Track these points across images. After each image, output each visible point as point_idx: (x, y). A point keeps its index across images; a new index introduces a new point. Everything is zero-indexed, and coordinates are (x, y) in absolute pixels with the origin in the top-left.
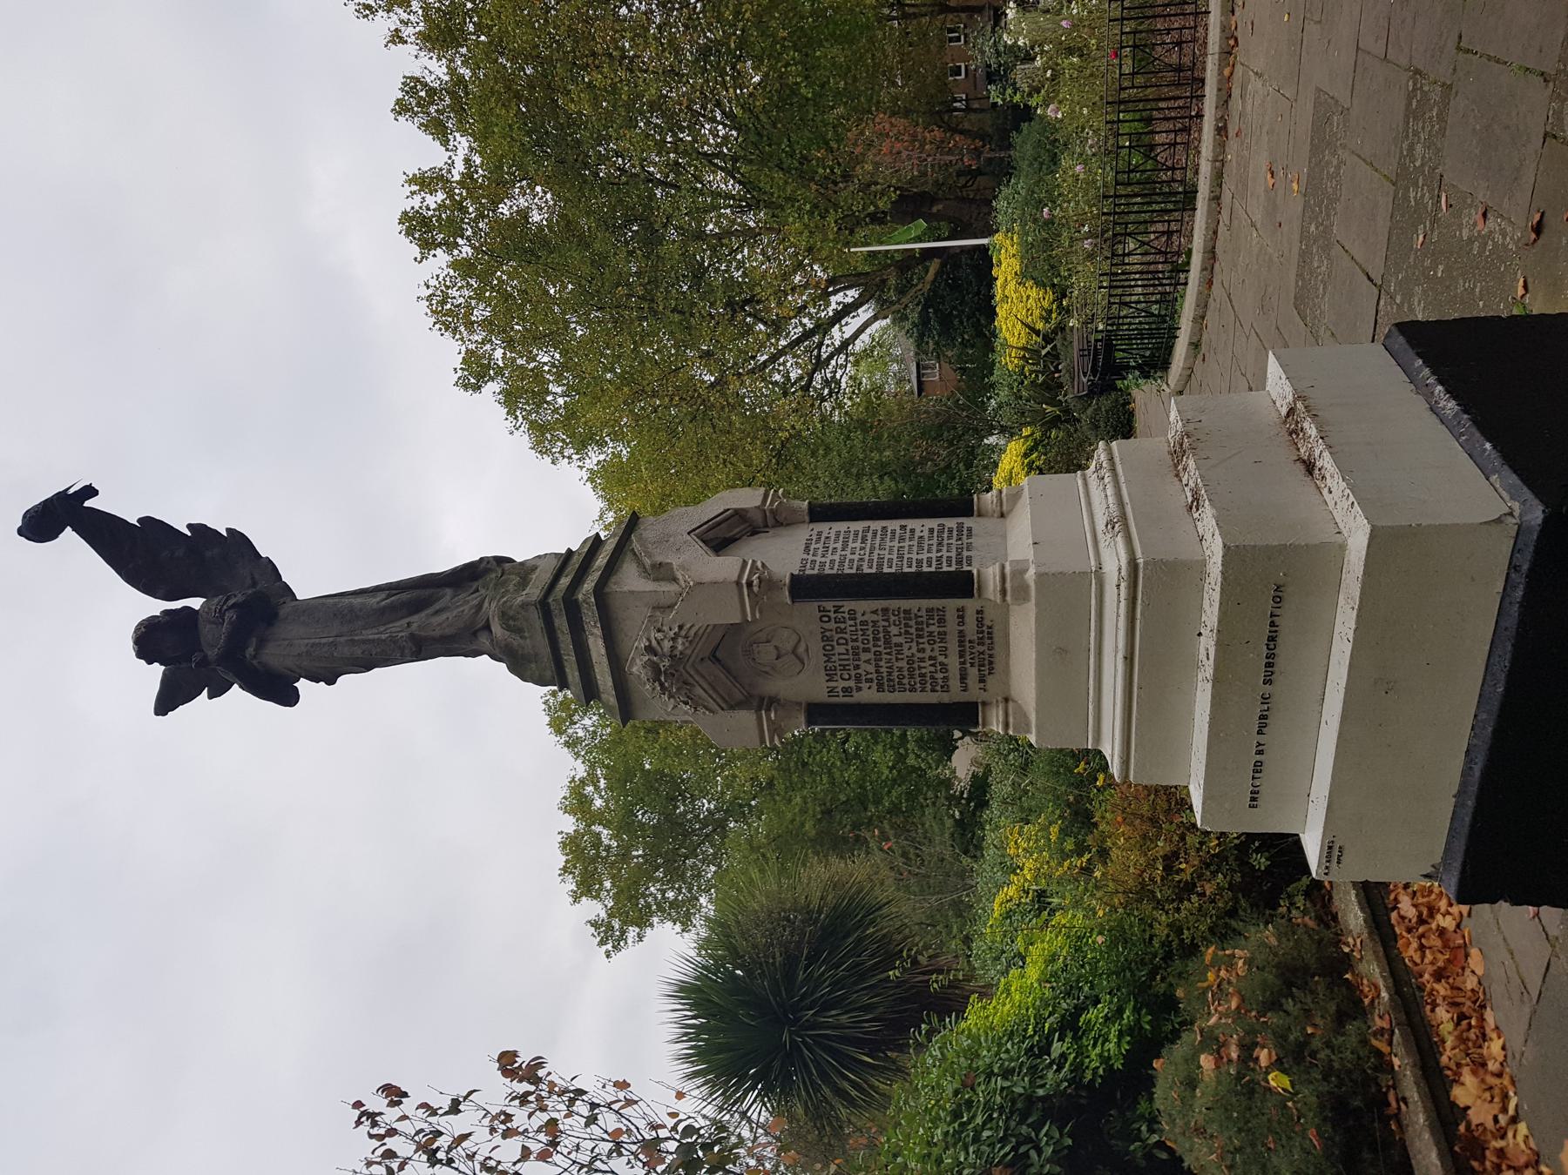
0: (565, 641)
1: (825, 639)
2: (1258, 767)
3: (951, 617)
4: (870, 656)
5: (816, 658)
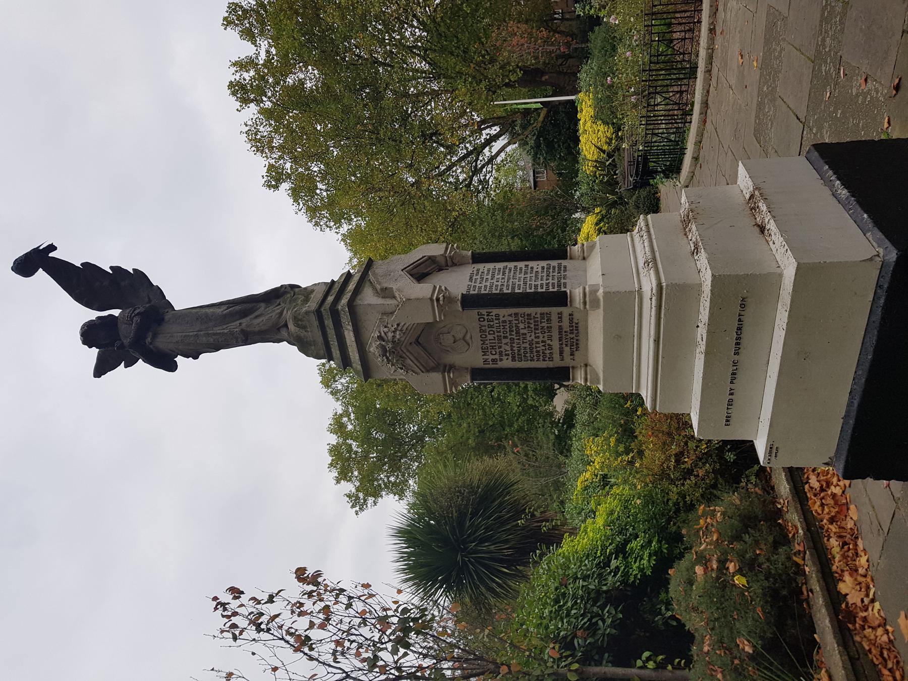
0: (331, 333)
2: (730, 403)
3: (555, 318)
4: (508, 340)
5: (477, 342)
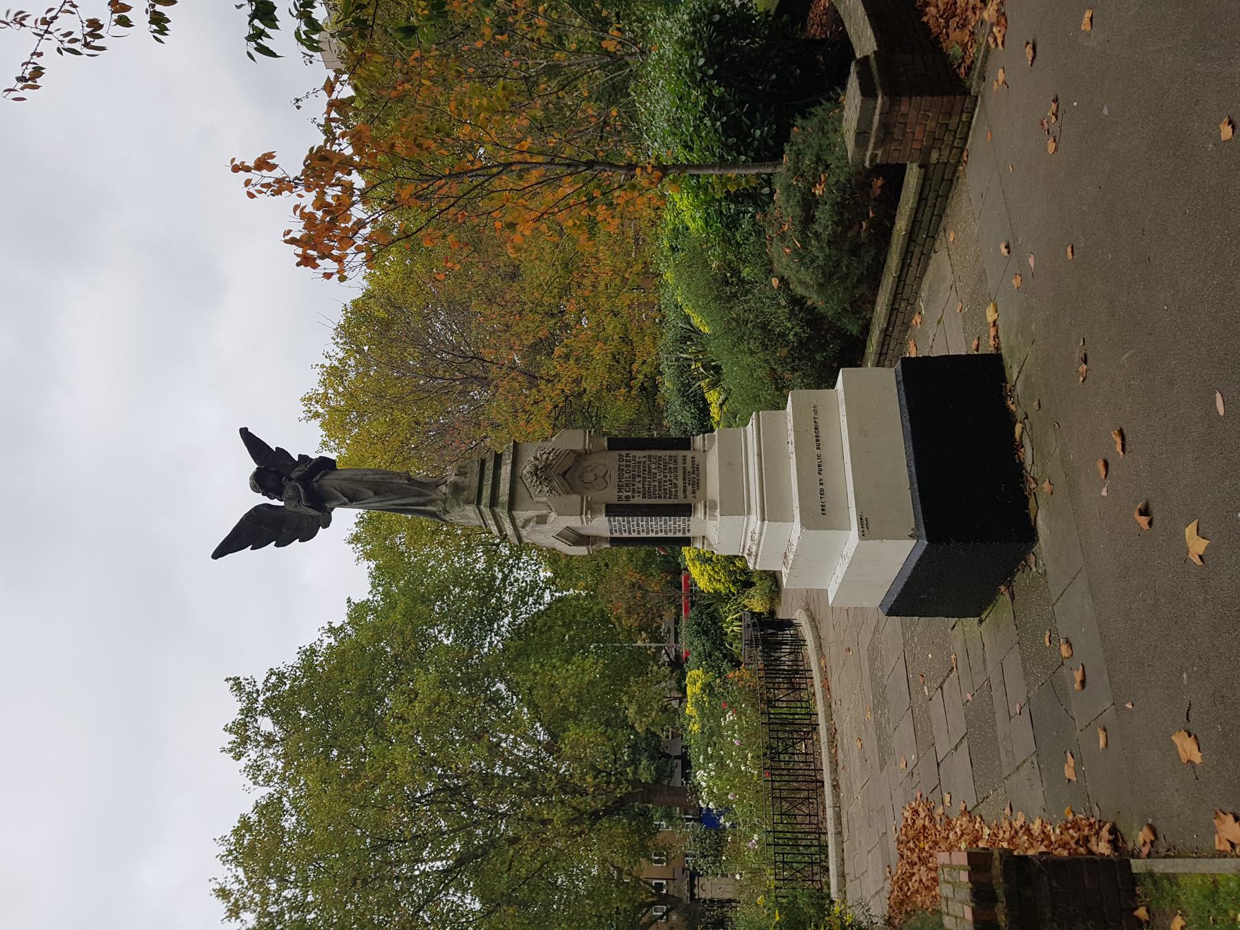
0: (489, 474)
2: (822, 492)
3: (680, 460)
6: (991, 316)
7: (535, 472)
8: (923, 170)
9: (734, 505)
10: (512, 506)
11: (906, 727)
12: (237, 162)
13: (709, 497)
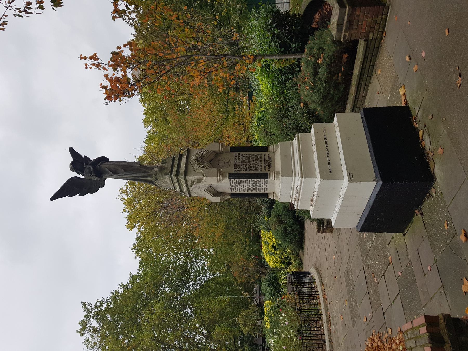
1: (235, 160)
2: (329, 164)
3: (263, 156)
6: (402, 91)
7: (197, 160)
8: (366, 42)
9: (288, 172)
10: (186, 174)
11: (366, 302)
12: (83, 56)
13: (276, 170)
